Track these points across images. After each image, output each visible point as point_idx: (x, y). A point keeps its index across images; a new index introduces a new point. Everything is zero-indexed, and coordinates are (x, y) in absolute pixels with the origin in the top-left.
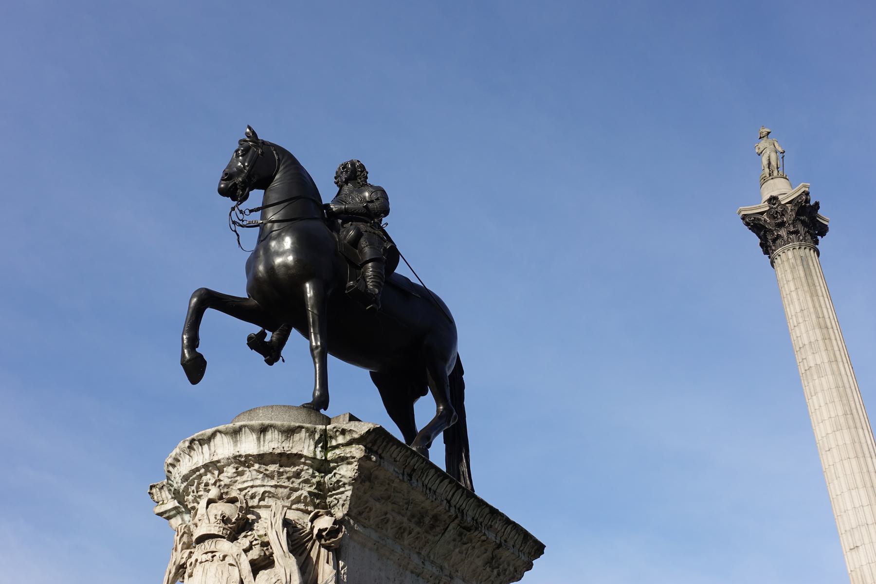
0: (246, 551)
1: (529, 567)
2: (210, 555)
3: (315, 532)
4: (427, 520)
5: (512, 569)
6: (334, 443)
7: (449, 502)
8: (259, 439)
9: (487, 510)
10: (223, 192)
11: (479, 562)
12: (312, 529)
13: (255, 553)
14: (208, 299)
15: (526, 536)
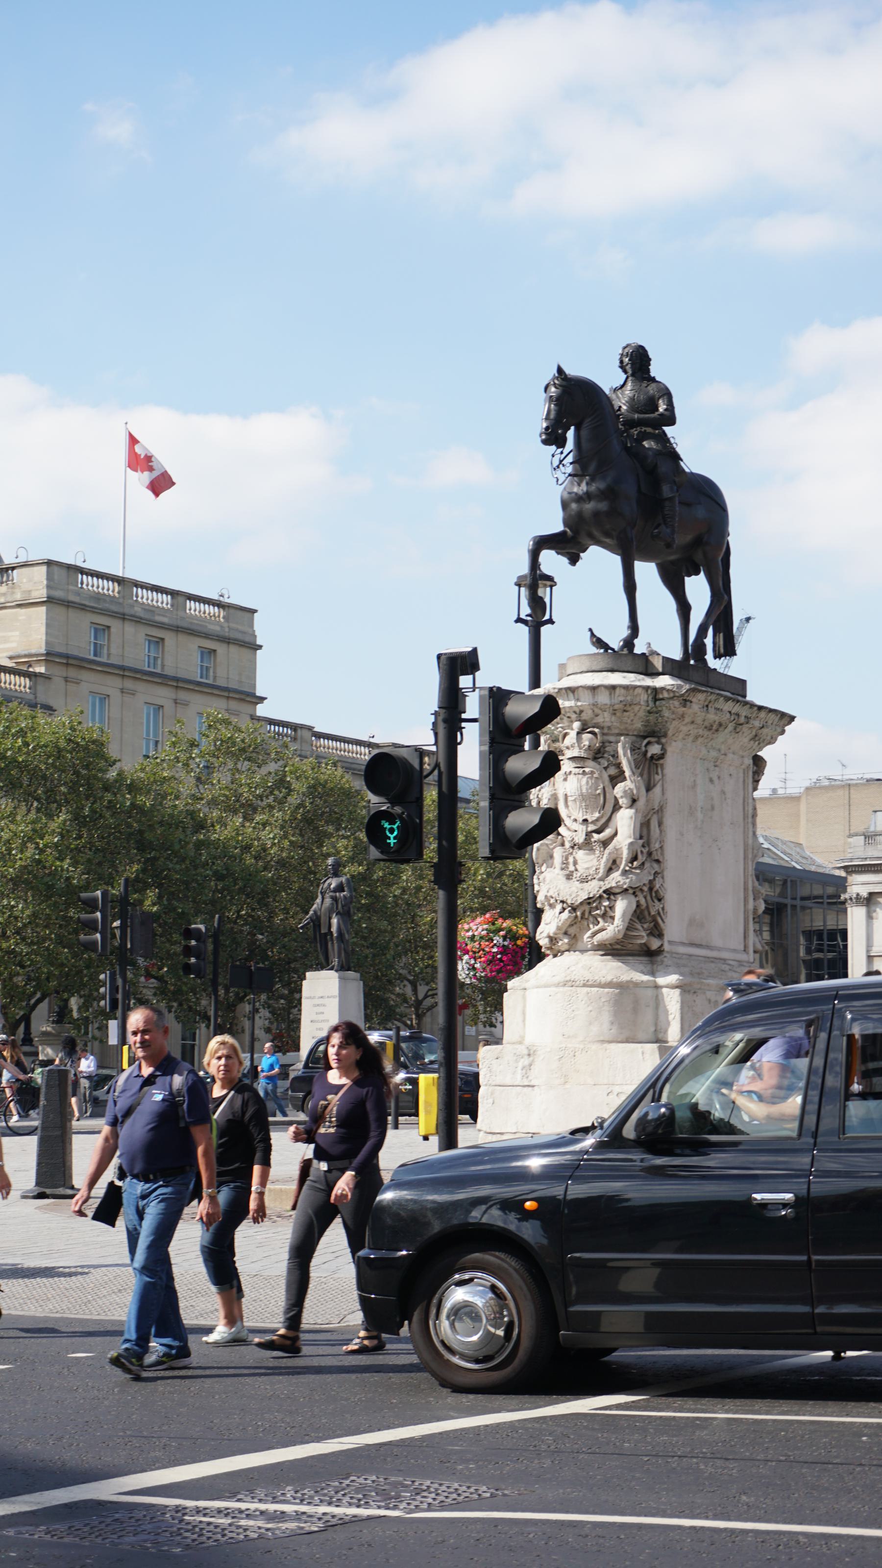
0: (606, 768)
1: (783, 732)
2: (582, 770)
3: (649, 755)
4: (715, 727)
5: (769, 738)
6: (661, 696)
7: (730, 712)
8: (610, 694)
9: (756, 708)
10: (546, 442)
11: (746, 740)
12: (646, 751)
13: (613, 771)
14: (542, 543)
15: (783, 715)
